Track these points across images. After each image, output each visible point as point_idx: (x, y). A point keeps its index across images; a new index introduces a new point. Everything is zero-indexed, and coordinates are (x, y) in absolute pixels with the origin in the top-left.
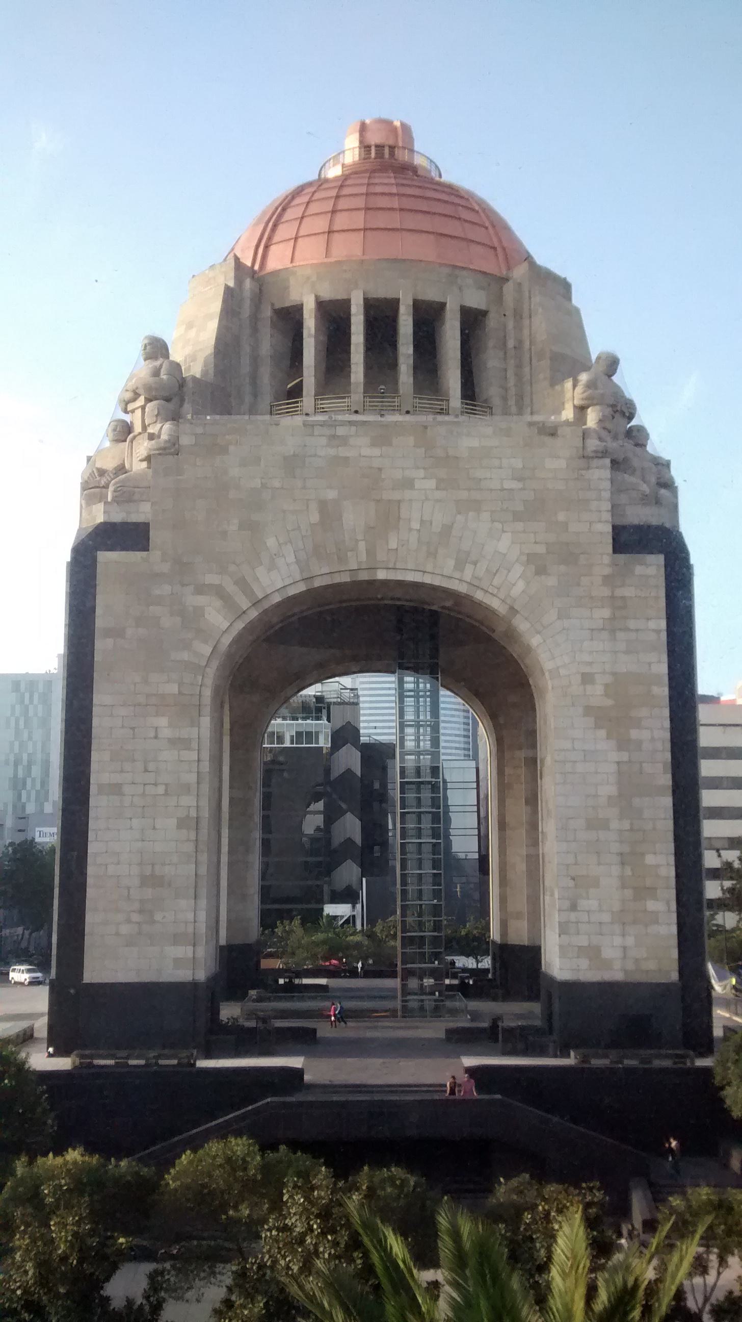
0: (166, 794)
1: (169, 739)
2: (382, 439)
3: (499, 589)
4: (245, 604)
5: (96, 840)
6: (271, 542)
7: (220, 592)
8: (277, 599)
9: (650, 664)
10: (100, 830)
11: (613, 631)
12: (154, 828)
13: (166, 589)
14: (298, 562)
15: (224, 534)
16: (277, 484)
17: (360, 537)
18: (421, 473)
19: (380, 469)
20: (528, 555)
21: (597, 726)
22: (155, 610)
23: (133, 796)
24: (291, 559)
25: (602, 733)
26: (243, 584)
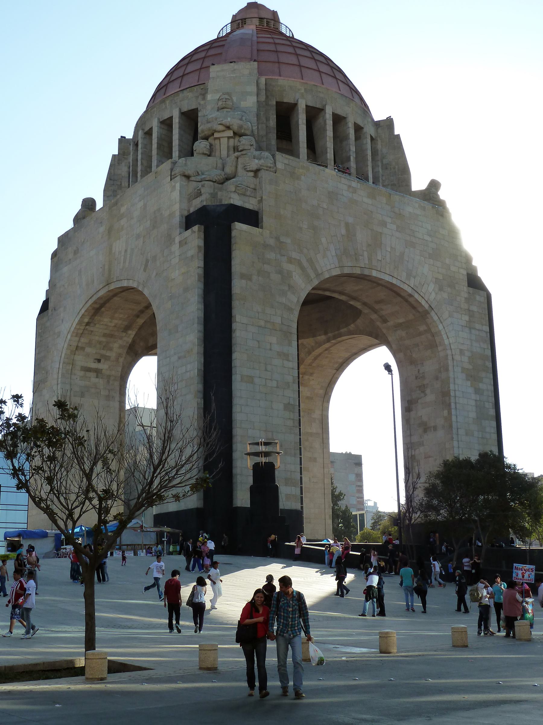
0: (277, 387)
1: (278, 352)
2: (372, 196)
3: (425, 294)
4: (313, 275)
5: (241, 412)
6: (323, 240)
7: (299, 264)
8: (327, 276)
9: (484, 349)
10: (243, 405)
11: (470, 328)
12: (272, 409)
13: (271, 255)
14: (337, 255)
15: (301, 229)
16: (325, 206)
17: (364, 249)
18: (389, 220)
19: (372, 212)
20: (436, 278)
21: (467, 380)
22: (267, 267)
23: (260, 385)
24: (334, 253)
25: (469, 383)
26: (310, 261)
